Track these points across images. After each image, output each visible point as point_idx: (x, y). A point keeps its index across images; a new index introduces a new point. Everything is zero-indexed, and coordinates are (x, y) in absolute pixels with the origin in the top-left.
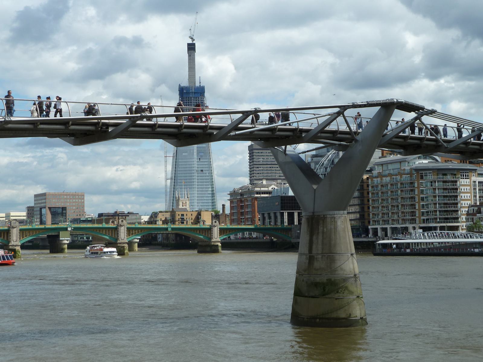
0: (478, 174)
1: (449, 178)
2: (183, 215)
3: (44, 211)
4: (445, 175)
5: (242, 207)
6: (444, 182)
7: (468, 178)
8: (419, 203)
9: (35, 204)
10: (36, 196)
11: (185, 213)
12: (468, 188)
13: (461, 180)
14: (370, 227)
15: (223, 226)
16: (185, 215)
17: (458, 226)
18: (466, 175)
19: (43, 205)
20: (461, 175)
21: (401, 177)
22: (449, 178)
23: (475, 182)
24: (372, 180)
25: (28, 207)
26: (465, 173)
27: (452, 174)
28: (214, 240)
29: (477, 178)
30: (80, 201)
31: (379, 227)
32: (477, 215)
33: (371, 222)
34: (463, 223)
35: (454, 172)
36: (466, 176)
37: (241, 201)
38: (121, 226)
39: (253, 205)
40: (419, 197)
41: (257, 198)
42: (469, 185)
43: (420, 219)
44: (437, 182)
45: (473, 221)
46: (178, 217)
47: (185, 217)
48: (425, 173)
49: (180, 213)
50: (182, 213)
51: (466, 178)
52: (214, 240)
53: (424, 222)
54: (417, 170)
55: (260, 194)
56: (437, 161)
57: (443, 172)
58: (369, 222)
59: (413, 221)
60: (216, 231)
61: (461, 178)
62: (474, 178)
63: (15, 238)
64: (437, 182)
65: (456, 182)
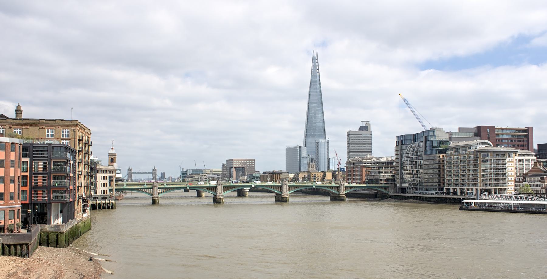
1: (499, 157)
3: (232, 170)
5: (354, 171)
6: (497, 160)
10: (227, 161)
14: (444, 188)
15: (347, 185)
17: (506, 189)
19: (231, 166)
22: (499, 157)
23: (516, 160)
26: (510, 154)
28: (341, 193)
31: (451, 188)
33: (446, 185)
34: (510, 187)
35: (503, 153)
37: (354, 168)
38: (285, 184)
39: (361, 171)
41: (364, 167)
43: (480, 184)
46: (312, 176)
47: (316, 176)
52: (341, 193)
54: (480, 152)
56: (491, 145)
57: (497, 153)
58: (444, 184)
59: (476, 185)
60: (342, 188)
62: (516, 157)
63: (220, 192)
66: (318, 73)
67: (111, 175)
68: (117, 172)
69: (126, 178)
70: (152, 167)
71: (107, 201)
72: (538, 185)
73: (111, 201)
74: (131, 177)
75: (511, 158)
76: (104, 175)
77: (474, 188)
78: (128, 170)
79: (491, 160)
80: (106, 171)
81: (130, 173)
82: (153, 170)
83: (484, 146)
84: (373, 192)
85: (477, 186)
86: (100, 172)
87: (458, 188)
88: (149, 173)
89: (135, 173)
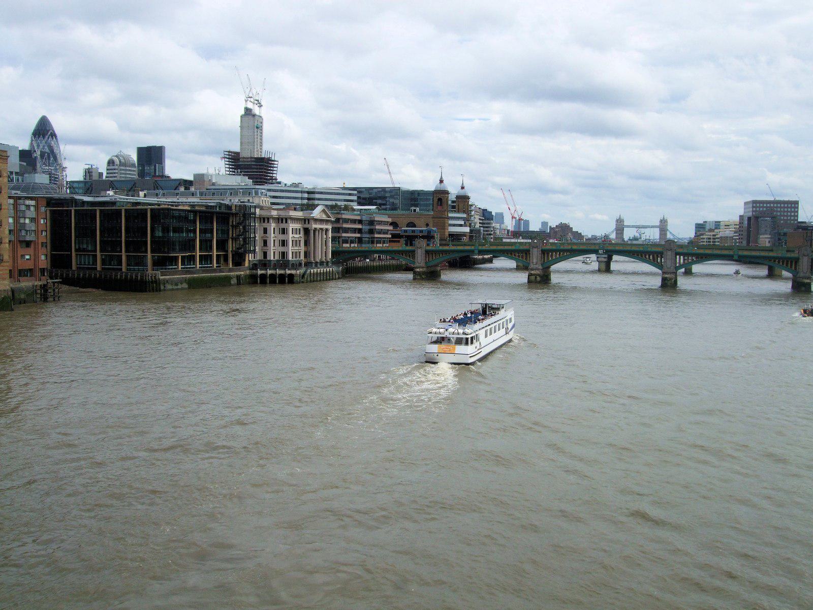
9: (745, 212)
25: (740, 216)
30: (793, 210)
63: (535, 261)
67: (306, 226)
68: (451, 222)
69: (613, 236)
70: (660, 217)
71: (279, 272)
73: (288, 272)
74: (622, 233)
76: (283, 225)
78: (617, 221)
80: (268, 219)
81: (620, 227)
82: (661, 221)
86: (271, 221)
88: (653, 227)
89: (628, 226)
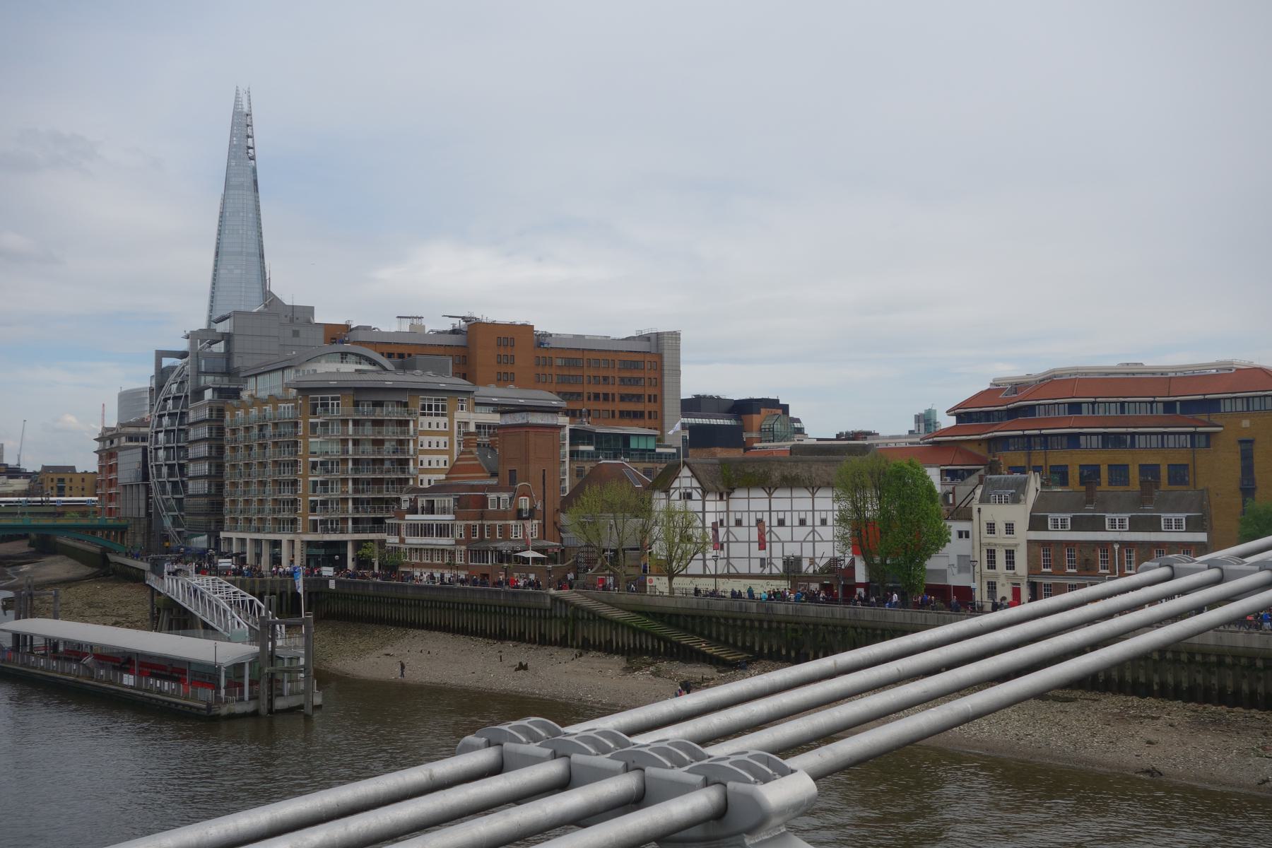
0: (477, 404)
2: (61, 480)
4: (378, 404)
6: (378, 423)
7: (443, 415)
8: (305, 476)
11: (67, 477)
12: (442, 440)
13: (421, 419)
14: (222, 535)
16: (67, 481)
18: (437, 406)
20: (423, 408)
21: (275, 408)
22: (390, 412)
24: (233, 415)
27: (399, 403)
29: (472, 415)
32: (408, 517)
33: (227, 523)
36: (437, 407)
40: (306, 462)
42: (449, 433)
43: (305, 519)
44: (351, 424)
45: (399, 534)
48: (322, 399)
49: (56, 477)
50: (61, 476)
51: (437, 415)
53: (315, 530)
55: (137, 440)
56: (385, 369)
61: (423, 415)
62: (460, 415)
64: (351, 424)
65: (406, 423)
66: (252, 158)
72: (443, 530)
75: (434, 420)
77: (285, 538)
79: (345, 422)
83: (349, 367)
84: (95, 549)
85: (294, 531)
87: (248, 536)
